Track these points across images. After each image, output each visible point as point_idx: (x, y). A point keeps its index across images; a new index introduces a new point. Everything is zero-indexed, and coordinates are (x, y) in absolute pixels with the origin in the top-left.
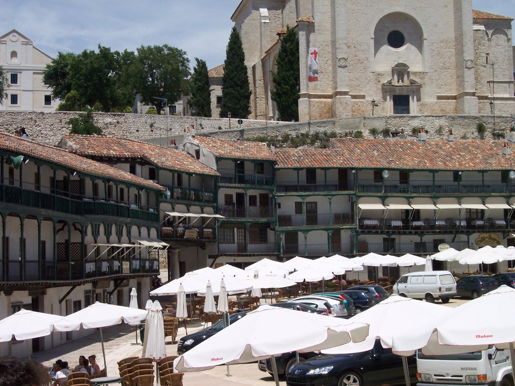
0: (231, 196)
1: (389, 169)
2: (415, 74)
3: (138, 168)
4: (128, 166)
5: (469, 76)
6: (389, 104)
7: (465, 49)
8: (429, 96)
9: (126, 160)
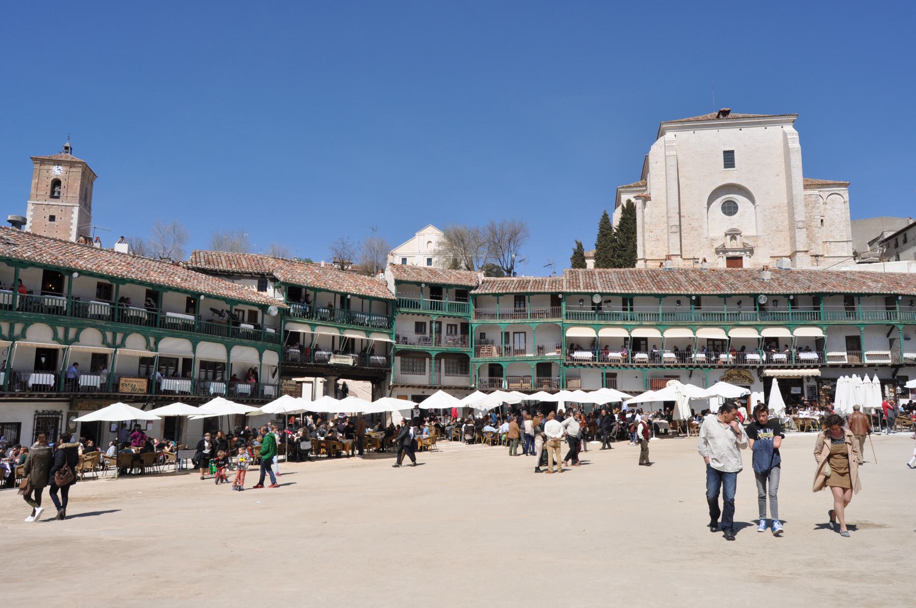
0: (425, 323)
1: (602, 294)
2: (746, 237)
4: (256, 281)
9: (251, 276)
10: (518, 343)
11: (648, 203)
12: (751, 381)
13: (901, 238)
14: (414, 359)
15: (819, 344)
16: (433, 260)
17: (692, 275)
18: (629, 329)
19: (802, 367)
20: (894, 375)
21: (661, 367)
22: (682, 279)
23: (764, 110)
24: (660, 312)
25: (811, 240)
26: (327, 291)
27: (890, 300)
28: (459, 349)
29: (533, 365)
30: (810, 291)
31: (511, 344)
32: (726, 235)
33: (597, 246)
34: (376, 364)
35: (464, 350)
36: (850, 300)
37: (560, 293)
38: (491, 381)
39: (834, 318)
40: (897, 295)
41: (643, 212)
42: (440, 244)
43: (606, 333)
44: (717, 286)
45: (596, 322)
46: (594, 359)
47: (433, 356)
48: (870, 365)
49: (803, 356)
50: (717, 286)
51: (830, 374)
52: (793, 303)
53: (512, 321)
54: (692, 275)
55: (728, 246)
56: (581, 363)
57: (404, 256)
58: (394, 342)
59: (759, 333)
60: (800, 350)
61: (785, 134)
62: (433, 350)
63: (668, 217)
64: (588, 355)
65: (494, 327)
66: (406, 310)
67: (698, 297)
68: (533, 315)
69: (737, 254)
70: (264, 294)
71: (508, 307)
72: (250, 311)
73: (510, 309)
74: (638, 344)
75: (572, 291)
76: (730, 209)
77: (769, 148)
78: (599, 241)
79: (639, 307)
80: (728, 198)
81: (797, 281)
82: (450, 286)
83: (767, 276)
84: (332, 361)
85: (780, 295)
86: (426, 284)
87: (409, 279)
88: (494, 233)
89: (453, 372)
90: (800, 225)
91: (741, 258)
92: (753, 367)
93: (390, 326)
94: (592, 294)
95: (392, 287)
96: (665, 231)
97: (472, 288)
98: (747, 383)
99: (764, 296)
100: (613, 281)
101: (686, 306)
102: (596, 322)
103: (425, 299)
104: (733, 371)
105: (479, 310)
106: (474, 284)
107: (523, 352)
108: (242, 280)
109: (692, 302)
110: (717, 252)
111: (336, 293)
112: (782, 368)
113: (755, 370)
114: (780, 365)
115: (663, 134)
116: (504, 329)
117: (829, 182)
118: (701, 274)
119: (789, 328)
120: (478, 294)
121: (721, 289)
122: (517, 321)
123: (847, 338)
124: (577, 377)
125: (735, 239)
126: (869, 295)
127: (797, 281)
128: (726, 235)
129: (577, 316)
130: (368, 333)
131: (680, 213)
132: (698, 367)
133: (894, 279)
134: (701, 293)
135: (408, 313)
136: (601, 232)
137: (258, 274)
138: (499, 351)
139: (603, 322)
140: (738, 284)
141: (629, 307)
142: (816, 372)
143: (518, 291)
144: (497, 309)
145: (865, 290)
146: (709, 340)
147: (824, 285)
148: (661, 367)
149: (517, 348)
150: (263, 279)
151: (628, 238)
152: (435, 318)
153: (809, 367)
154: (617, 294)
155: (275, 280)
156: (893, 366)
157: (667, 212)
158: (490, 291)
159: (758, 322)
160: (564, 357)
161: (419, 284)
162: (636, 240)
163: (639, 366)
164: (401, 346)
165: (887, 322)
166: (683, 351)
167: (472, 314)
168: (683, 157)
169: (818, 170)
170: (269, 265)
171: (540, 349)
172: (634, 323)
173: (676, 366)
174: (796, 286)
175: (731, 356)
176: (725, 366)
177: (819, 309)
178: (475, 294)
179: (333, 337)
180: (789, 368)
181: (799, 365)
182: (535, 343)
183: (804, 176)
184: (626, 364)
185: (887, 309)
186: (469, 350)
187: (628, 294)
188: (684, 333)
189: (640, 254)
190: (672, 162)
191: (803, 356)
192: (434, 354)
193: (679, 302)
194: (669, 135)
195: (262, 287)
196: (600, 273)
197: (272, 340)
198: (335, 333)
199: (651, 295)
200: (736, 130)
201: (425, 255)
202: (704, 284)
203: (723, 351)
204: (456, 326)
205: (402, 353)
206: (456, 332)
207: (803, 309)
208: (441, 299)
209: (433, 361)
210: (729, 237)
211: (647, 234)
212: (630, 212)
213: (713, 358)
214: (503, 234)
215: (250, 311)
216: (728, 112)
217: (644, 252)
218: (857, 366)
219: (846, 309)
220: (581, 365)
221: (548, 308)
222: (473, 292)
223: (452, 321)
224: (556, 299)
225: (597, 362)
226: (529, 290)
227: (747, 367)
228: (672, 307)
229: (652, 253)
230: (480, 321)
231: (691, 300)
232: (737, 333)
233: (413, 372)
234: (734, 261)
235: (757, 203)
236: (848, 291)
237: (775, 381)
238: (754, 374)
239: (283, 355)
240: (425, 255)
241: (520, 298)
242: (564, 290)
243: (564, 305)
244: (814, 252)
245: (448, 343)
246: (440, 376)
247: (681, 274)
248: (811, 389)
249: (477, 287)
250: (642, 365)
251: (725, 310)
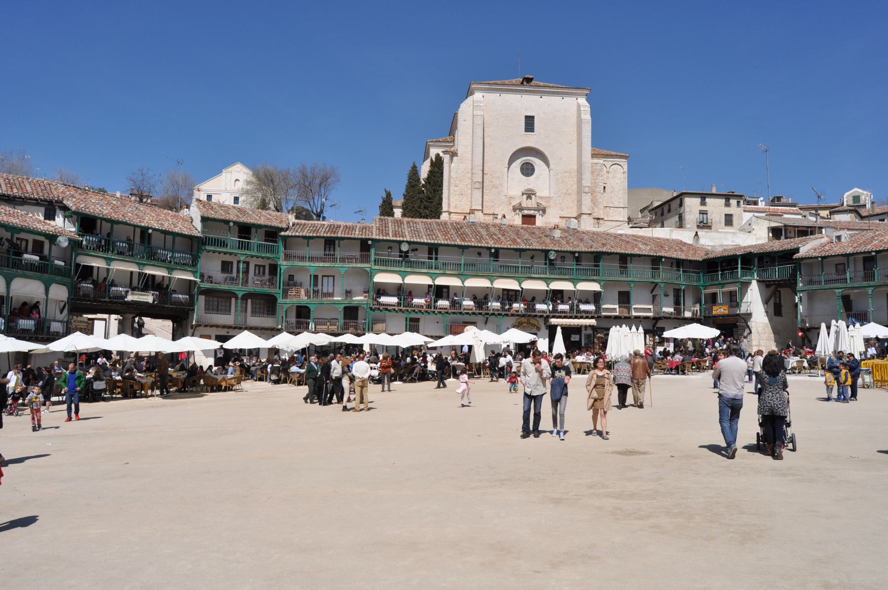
1: (409, 243)
2: (540, 198)
4: (43, 209)
5: (587, 200)
7: (583, 177)
9: (37, 202)
10: (326, 286)
11: (455, 158)
12: (538, 329)
13: (666, 208)
14: (219, 299)
15: (596, 297)
16: (241, 199)
17: (492, 229)
18: (433, 277)
19: (582, 317)
20: (654, 326)
21: (461, 313)
22: (484, 232)
23: (563, 82)
24: (463, 262)
25: (594, 204)
26: (126, 224)
27: (656, 261)
28: (266, 290)
29: (341, 308)
30: (592, 250)
31: (320, 287)
32: (523, 194)
33: (405, 196)
34: (178, 302)
35: (272, 291)
36: (624, 259)
37: (369, 239)
38: (297, 322)
39: (610, 275)
40: (661, 257)
41: (450, 167)
42: (248, 183)
43: (411, 280)
44: (514, 241)
45: (402, 269)
46: (399, 304)
47: (240, 296)
48: (637, 317)
49: (583, 307)
50: (514, 241)
51: (604, 324)
52: (578, 260)
53: (321, 264)
54: (492, 229)
55: (524, 205)
56: (387, 307)
57: (209, 193)
58: (198, 280)
59: (548, 285)
60: (580, 301)
61: (579, 106)
62: (240, 289)
63: (472, 174)
64: (394, 300)
65: (303, 269)
66: (212, 248)
67: (497, 249)
68: (343, 260)
69: (532, 212)
70: (52, 222)
71: (318, 250)
72: (35, 241)
73: (320, 253)
74: (440, 292)
75: (381, 237)
76: (528, 170)
77: (564, 115)
78: (407, 191)
79: (443, 257)
80: (527, 159)
81: (582, 240)
82: (260, 226)
83: (557, 234)
84: (130, 298)
85: (567, 252)
86: (235, 223)
87: (217, 216)
88: (305, 176)
89: (260, 313)
90: (586, 190)
91: (535, 216)
92: (541, 316)
93: (194, 264)
94: (400, 242)
95: (198, 225)
96: (469, 186)
97: (282, 229)
98: (535, 331)
99: (553, 253)
100: (418, 231)
101: (486, 258)
102: (402, 269)
103: (233, 238)
104: (523, 320)
105: (288, 251)
106: (284, 226)
107: (331, 295)
108: (26, 207)
109: (491, 255)
110: (514, 209)
111: (135, 226)
112: (565, 317)
113: (542, 319)
114: (564, 315)
115: (472, 94)
116: (313, 272)
117: (613, 153)
118: (500, 229)
119: (573, 283)
120: (288, 236)
121: (518, 243)
122: (326, 265)
123: (620, 293)
124: (383, 321)
125: (531, 199)
126: (639, 256)
127: (582, 240)
128: (523, 194)
129: (385, 263)
130: (170, 270)
131: (483, 170)
132: (493, 314)
133: (660, 243)
134: (499, 246)
135: (214, 252)
136: (410, 183)
137: (45, 200)
138: (307, 293)
139: (409, 270)
140: (532, 240)
141: (434, 256)
142: (593, 322)
143: (329, 235)
144: (307, 252)
145: (636, 251)
146: (504, 290)
147: (604, 245)
148: (461, 313)
149: (325, 291)
150: (51, 208)
151: (435, 191)
152: (242, 258)
153: (587, 318)
154: (424, 244)
155: (65, 208)
156: (654, 318)
157: (472, 169)
158: (301, 234)
159: (548, 276)
160: (370, 301)
161: (227, 222)
162: (442, 193)
163: (440, 313)
164: (206, 285)
165: (652, 280)
166: (481, 298)
167: (282, 255)
168: (489, 116)
169: (605, 141)
170: (58, 191)
171: (348, 293)
172: (438, 272)
173: (474, 313)
174: (581, 244)
175: (522, 305)
176: (517, 314)
177: (598, 266)
178: (284, 236)
179: (132, 273)
180: (571, 317)
181: (579, 315)
182: (342, 287)
183: (592, 146)
184: (429, 310)
185: (653, 269)
186: (277, 291)
187: (434, 244)
188: (482, 283)
189: (445, 207)
190: (479, 121)
191: (583, 307)
192: (240, 294)
193: (479, 254)
194: (478, 96)
195: (50, 215)
196: (408, 223)
197: (61, 275)
198: (134, 269)
199: (455, 246)
200: (535, 98)
201: (232, 193)
202: (503, 238)
203: (516, 301)
204: (264, 267)
205: (206, 292)
206: (264, 273)
207: (586, 265)
208: (249, 239)
209: (239, 301)
210: (525, 196)
211: (452, 188)
212: (437, 165)
213: (507, 307)
214: (314, 178)
215: (35, 241)
216: (531, 79)
217: (449, 205)
218: (626, 318)
219: (621, 267)
220: (386, 309)
221: (357, 254)
222: (283, 233)
223: (260, 262)
224: (365, 245)
225: (402, 308)
226: (339, 235)
227: (536, 316)
228: (473, 258)
229: (456, 207)
230: (290, 263)
231: (491, 252)
232: (529, 285)
233: (218, 311)
234: (529, 219)
235: (551, 167)
236: (623, 251)
237: (559, 329)
238: (541, 322)
239: (74, 291)
240: (232, 193)
241: (330, 243)
242: (374, 237)
243: (373, 251)
244: (596, 215)
245: (255, 284)
246: (246, 317)
247: (483, 228)
248: (588, 337)
249: (287, 229)
250: (444, 312)
251: (520, 263)
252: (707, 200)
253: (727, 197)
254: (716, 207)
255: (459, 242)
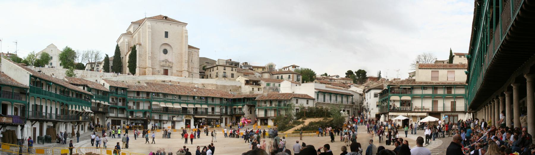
3: (86, 88)
6: (162, 72)
8: (175, 70)
69: (166, 68)
76: (165, 52)
95: (108, 88)
127: (202, 92)
155: (87, 86)
195: (84, 89)
252: (226, 68)
253: (232, 67)
254: (229, 71)
255: (171, 93)
